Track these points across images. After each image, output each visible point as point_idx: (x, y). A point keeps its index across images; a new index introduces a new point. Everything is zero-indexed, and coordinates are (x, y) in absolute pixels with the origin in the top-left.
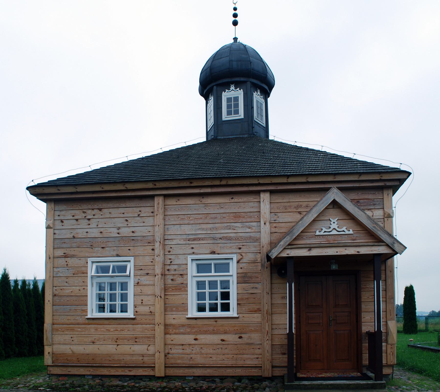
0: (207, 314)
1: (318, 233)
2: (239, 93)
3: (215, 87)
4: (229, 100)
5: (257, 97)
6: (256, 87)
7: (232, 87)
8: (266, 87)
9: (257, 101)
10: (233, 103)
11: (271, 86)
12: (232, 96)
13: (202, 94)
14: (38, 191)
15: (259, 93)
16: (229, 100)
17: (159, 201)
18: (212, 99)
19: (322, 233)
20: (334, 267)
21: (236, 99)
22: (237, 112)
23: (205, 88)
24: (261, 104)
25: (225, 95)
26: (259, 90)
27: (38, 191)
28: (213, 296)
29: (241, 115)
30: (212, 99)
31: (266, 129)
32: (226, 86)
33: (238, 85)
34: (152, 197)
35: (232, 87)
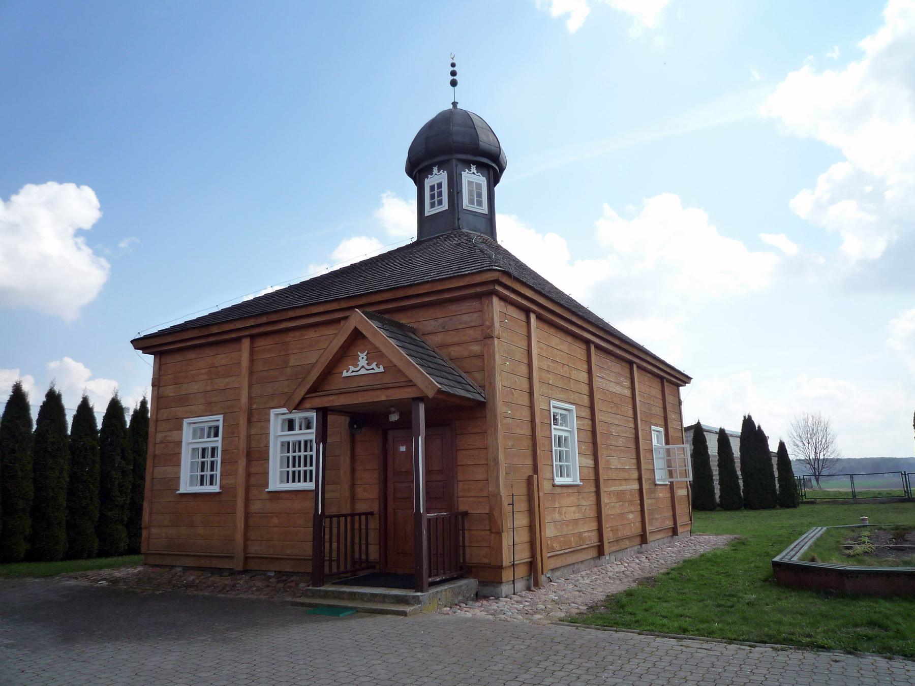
1: (345, 374)
6: (467, 164)
9: (470, 183)
12: (435, 183)
14: (143, 344)
16: (432, 188)
17: (246, 343)
19: (349, 374)
21: (440, 185)
22: (440, 203)
24: (479, 186)
25: (428, 182)
27: (143, 344)
29: (445, 206)
31: (490, 219)
32: (428, 171)
33: (442, 165)
34: (238, 340)
35: (435, 170)
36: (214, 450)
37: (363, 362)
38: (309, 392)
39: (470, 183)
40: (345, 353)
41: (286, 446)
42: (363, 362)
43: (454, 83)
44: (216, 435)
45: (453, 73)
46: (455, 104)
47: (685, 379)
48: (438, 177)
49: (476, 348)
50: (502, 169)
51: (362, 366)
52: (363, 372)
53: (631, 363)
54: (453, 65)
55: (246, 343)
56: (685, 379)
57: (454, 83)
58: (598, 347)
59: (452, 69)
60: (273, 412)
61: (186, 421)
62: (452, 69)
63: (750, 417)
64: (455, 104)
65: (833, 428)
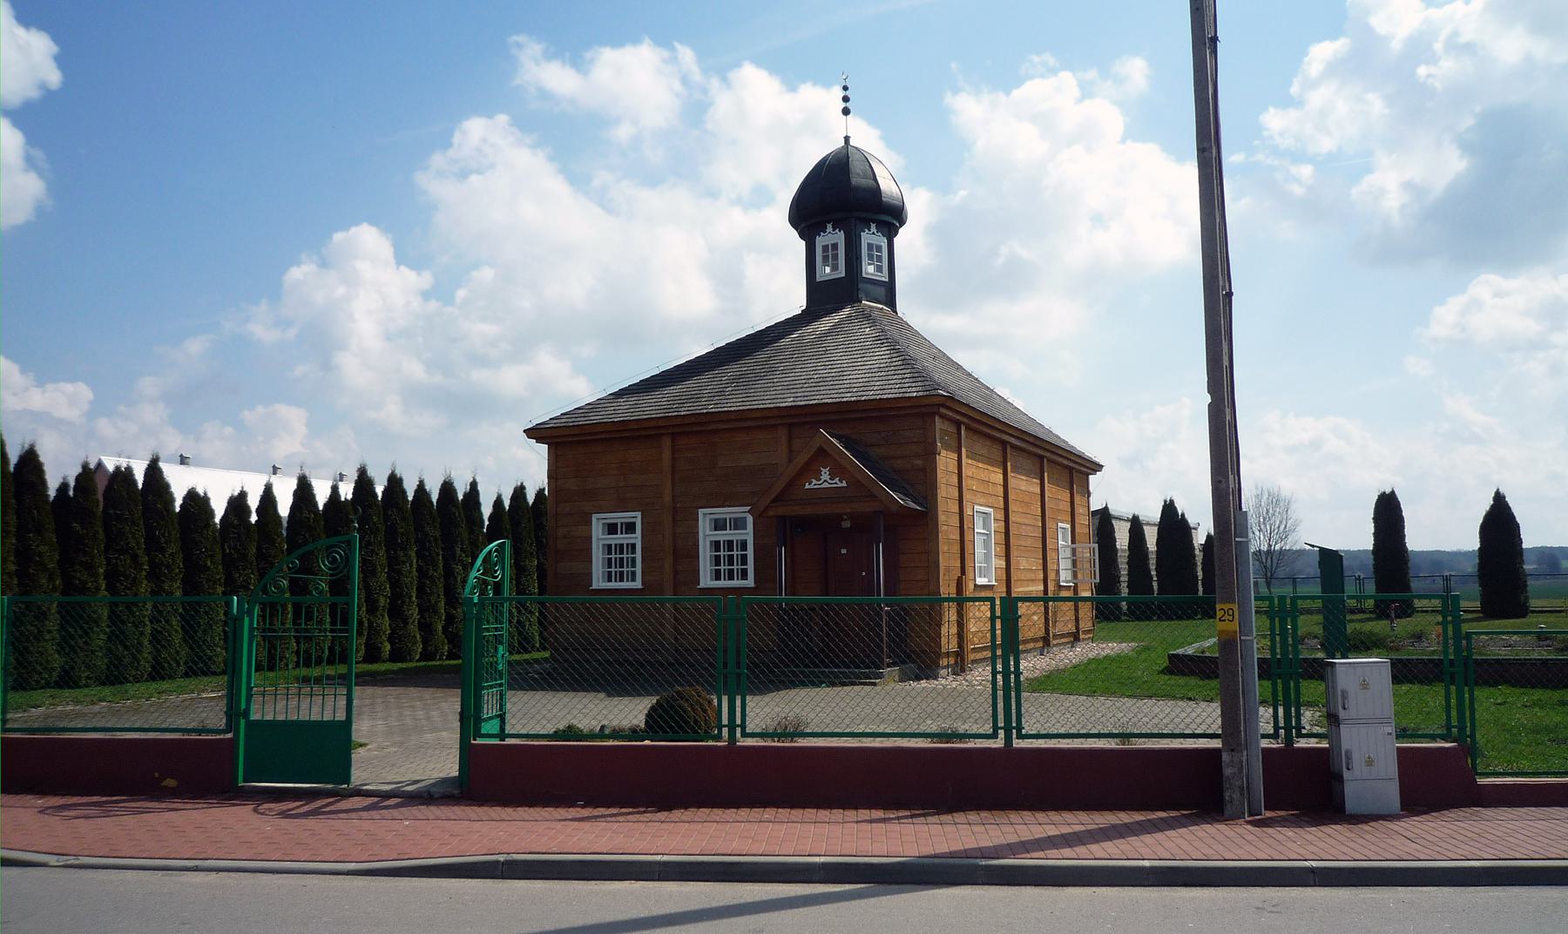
0: (724, 583)
2: (839, 237)
6: (866, 223)
7: (829, 227)
9: (870, 246)
10: (830, 252)
15: (873, 228)
16: (825, 248)
17: (667, 443)
20: (847, 524)
21: (835, 246)
24: (879, 248)
25: (821, 241)
28: (731, 560)
29: (841, 273)
35: (829, 227)
36: (633, 546)
37: (825, 474)
38: (774, 501)
39: (870, 246)
40: (810, 469)
41: (716, 545)
42: (825, 474)
44: (633, 531)
45: (846, 99)
46: (847, 139)
47: (1096, 467)
48: (833, 237)
49: (919, 462)
50: (902, 223)
51: (825, 480)
52: (826, 485)
53: (1042, 458)
54: (845, 88)
55: (667, 443)
56: (1096, 467)
57: (846, 112)
58: (1014, 447)
60: (701, 511)
61: (594, 517)
63: (1172, 502)
64: (847, 139)
65: (1297, 512)
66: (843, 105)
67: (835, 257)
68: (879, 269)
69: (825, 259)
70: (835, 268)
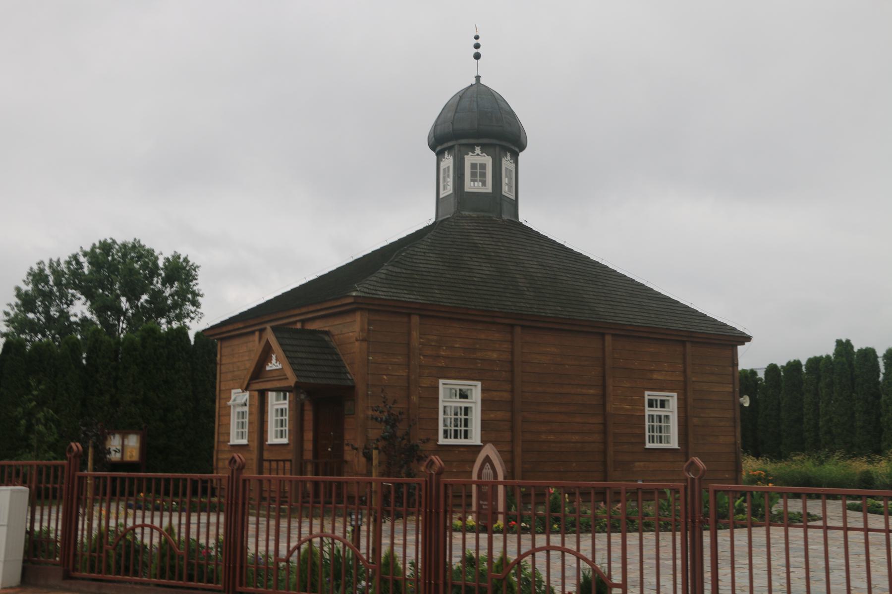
2: (488, 160)
3: (456, 147)
4: (474, 166)
5: (507, 163)
6: (506, 150)
7: (478, 150)
8: (517, 150)
10: (478, 172)
11: (522, 147)
13: (433, 147)
15: (509, 158)
16: (474, 166)
18: (448, 161)
21: (483, 166)
23: (441, 144)
25: (469, 159)
26: (509, 154)
29: (489, 189)
30: (448, 161)
31: (515, 204)
32: (471, 147)
33: (485, 148)
35: (478, 150)
43: (477, 56)
45: (477, 46)
46: (478, 78)
54: (477, 38)
57: (477, 56)
59: (475, 41)
62: (475, 41)
64: (478, 78)
66: (475, 50)
67: (483, 175)
68: (510, 190)
69: (473, 175)
70: (484, 184)
